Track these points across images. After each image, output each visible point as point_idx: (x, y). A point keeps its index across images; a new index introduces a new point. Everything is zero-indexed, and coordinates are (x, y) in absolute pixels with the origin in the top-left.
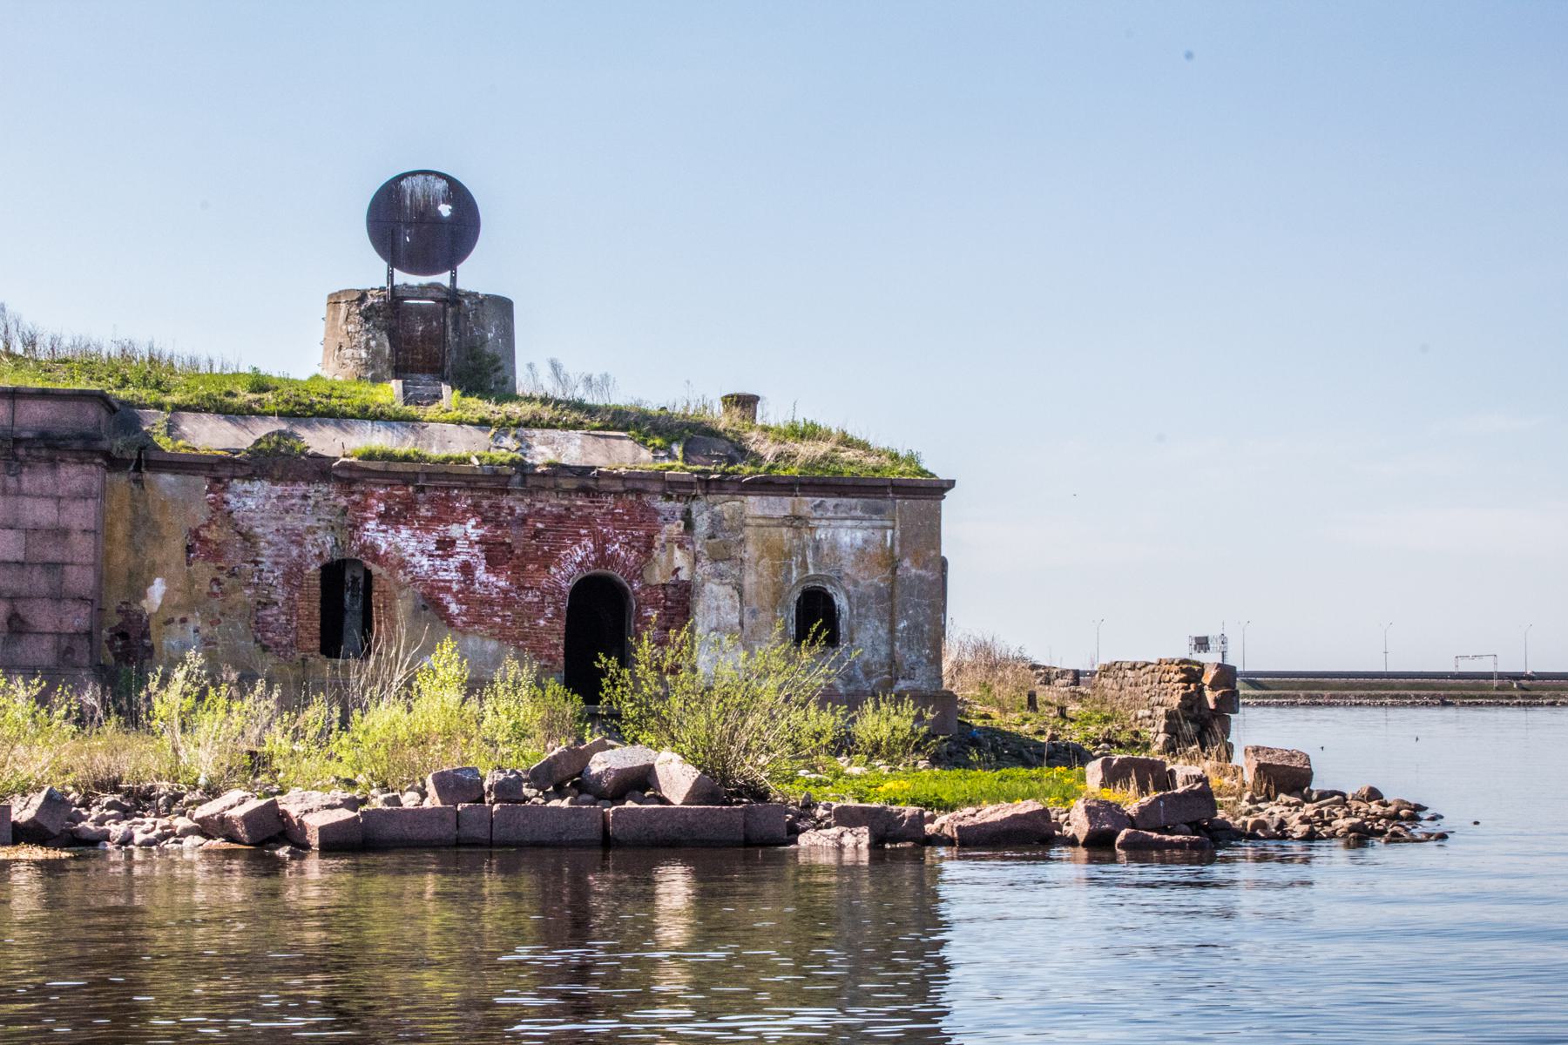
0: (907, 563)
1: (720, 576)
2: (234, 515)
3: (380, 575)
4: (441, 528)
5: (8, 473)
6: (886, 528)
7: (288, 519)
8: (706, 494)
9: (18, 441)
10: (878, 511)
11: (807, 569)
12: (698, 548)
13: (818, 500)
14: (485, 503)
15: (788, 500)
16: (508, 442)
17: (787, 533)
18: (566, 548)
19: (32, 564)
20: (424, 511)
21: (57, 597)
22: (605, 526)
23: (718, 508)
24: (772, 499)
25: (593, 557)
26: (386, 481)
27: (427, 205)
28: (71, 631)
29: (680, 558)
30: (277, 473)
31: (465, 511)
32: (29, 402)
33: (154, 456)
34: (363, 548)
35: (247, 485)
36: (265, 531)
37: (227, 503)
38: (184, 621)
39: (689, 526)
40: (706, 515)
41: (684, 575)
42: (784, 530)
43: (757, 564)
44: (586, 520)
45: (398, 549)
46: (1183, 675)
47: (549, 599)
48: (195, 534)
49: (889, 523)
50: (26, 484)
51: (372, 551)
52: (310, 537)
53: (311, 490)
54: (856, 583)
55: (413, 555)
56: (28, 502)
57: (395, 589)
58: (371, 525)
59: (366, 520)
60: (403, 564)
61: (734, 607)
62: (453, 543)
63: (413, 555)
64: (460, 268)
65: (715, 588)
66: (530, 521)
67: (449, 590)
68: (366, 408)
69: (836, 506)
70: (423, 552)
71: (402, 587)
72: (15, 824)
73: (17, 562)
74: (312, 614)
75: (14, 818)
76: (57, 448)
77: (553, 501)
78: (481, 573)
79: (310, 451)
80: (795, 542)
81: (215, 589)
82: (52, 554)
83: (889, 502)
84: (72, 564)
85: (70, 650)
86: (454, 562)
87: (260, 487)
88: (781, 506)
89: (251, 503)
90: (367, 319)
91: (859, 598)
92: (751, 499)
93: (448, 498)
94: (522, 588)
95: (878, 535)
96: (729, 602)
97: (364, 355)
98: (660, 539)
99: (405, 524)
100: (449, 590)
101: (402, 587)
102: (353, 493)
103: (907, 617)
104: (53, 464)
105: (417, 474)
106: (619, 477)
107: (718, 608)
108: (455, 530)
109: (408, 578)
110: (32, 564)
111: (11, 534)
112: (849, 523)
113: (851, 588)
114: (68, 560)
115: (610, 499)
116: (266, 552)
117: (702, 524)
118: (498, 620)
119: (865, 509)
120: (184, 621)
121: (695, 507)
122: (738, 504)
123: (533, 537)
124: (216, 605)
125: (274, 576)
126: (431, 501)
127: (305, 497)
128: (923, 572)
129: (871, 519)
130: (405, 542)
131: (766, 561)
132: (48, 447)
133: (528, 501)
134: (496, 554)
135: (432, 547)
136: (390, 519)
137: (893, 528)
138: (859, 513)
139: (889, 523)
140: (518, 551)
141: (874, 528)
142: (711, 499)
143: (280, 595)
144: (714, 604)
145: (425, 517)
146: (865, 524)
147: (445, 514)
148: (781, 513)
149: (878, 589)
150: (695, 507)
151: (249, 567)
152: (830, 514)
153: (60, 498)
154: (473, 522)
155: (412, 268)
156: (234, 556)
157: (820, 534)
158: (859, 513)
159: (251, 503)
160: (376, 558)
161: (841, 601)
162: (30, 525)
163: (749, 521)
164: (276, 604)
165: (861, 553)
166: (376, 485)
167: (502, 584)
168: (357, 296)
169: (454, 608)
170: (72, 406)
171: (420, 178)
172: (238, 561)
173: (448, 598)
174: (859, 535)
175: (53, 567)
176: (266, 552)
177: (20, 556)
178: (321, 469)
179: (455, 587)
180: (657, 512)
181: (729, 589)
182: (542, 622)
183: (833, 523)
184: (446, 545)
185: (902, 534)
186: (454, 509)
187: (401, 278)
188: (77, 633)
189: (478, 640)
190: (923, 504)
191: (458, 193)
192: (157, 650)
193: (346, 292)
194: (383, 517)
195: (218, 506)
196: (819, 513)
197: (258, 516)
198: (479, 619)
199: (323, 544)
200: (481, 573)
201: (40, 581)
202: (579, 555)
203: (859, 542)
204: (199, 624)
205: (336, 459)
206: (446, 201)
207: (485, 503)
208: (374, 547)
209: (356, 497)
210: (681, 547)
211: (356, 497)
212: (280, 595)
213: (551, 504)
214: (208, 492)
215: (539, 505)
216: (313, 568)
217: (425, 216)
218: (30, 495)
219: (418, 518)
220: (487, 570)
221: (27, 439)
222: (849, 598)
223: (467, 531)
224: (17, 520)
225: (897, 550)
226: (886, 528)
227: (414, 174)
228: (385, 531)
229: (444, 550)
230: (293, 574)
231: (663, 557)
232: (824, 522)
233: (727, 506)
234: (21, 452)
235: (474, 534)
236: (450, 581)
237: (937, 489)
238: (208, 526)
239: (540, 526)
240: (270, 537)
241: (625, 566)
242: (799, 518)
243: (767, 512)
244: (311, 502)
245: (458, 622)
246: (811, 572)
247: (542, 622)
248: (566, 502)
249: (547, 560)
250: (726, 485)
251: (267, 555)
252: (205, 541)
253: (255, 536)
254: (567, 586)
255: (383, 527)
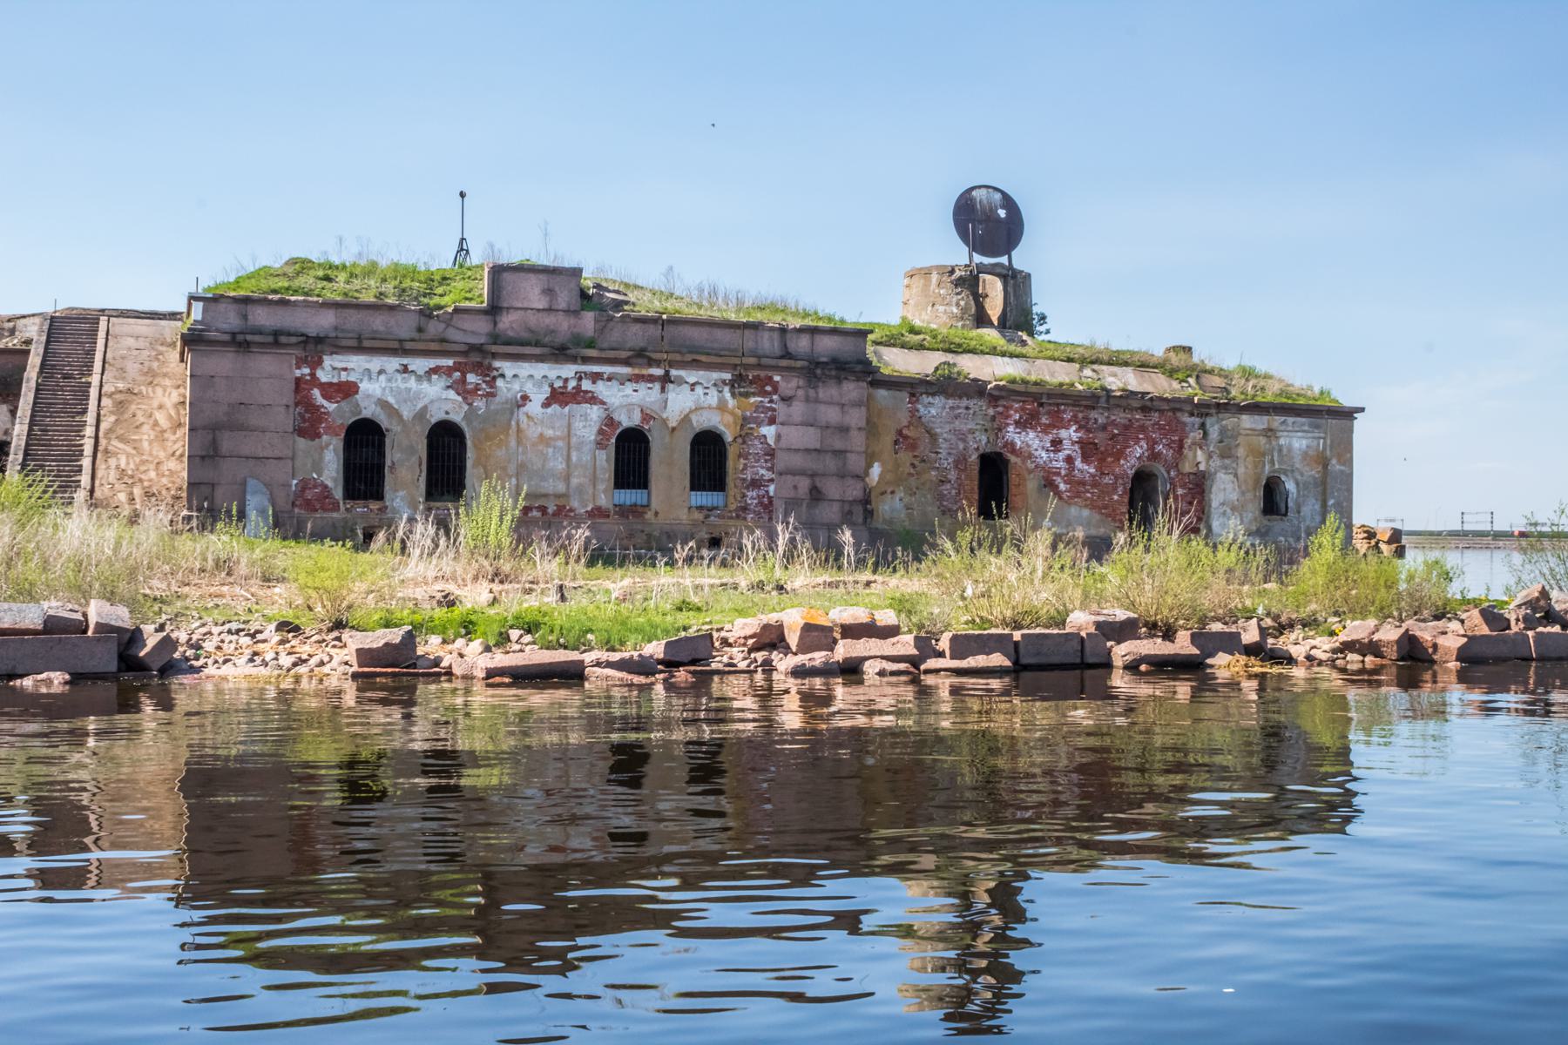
0: (1334, 461)
1: (1226, 468)
2: (923, 419)
3: (1016, 463)
4: (1055, 431)
5: (809, 386)
6: (1320, 438)
7: (957, 423)
8: (1217, 413)
9: (818, 364)
10: (1317, 427)
11: (1274, 464)
12: (1211, 449)
13: (1283, 418)
14: (1080, 415)
15: (1266, 418)
16: (1087, 372)
17: (1263, 440)
18: (1129, 447)
19: (826, 452)
20: (1044, 420)
21: (842, 475)
22: (1154, 432)
23: (1224, 422)
24: (1256, 417)
25: (1146, 454)
26: (1023, 399)
27: (991, 209)
28: (851, 499)
29: (1200, 456)
30: (950, 391)
31: (1070, 421)
32: (822, 337)
33: (878, 377)
34: (1006, 444)
35: (930, 399)
36: (942, 430)
37: (918, 411)
38: (893, 492)
39: (1205, 434)
40: (1216, 427)
41: (1202, 467)
42: (1261, 438)
43: (1245, 460)
44: (1143, 429)
45: (1028, 446)
46: (1366, 535)
47: (1120, 481)
48: (900, 433)
49: (1322, 435)
50: (821, 395)
51: (1010, 445)
52: (970, 436)
53: (971, 403)
54: (1302, 475)
55: (1036, 450)
56: (822, 408)
57: (1025, 473)
58: (1011, 429)
59: (1008, 425)
60: (1030, 456)
61: (1234, 489)
62: (1060, 442)
63: (1036, 450)
64: (1014, 253)
65: (1223, 476)
66: (1109, 428)
67: (1058, 474)
68: (995, 348)
69: (1294, 423)
70: (1043, 448)
71: (1030, 472)
72: (1245, 645)
73: (816, 450)
74: (973, 489)
75: (1244, 642)
76: (844, 369)
77: (1122, 415)
78: (1078, 463)
79: (971, 376)
80: (1267, 446)
81: (912, 471)
82: (838, 444)
83: (1324, 421)
84: (851, 452)
85: (850, 513)
86: (1061, 455)
87: (938, 401)
88: (1260, 422)
89: (933, 412)
90: (956, 286)
91: (1304, 485)
92: (1244, 417)
93: (1058, 411)
94: (1103, 474)
95: (1315, 442)
96: (1231, 485)
97: (955, 310)
98: (1188, 441)
99: (1031, 428)
100: (1058, 474)
101: (1030, 472)
102: (997, 406)
103: (1333, 498)
104: (839, 380)
105: (1042, 394)
106: (1166, 400)
107: (1225, 489)
108: (1063, 433)
109: (1033, 465)
110: (826, 452)
111: (811, 429)
112: (1299, 434)
113: (1299, 477)
114: (849, 448)
115: (1157, 415)
116: (944, 446)
117: (1214, 433)
118: (1089, 495)
119: (1310, 425)
120: (893, 492)
121: (1209, 421)
122: (1236, 420)
123: (1111, 439)
124: (913, 482)
125: (947, 462)
126: (1048, 413)
127: (967, 408)
128: (1342, 468)
129: (1313, 432)
130: (1031, 441)
131: (1250, 459)
132: (837, 369)
133: (1106, 414)
134: (1088, 449)
135: (1049, 445)
136: (1022, 425)
137: (1324, 438)
138: (1306, 428)
139: (1322, 435)
140: (1102, 449)
141: (1314, 438)
142: (1221, 416)
143: (952, 476)
144: (1222, 487)
145: (1045, 424)
146: (1310, 435)
147: (1058, 423)
148: (1262, 427)
149: (1315, 478)
150: (1209, 421)
151: (933, 455)
152: (1290, 428)
153: (843, 405)
154: (1074, 428)
155: (984, 253)
156: (924, 448)
157: (1282, 441)
158: (1306, 428)
159: (933, 412)
160: (1014, 451)
161: (1290, 486)
162: (824, 424)
163: (1242, 431)
164: (950, 482)
165: (1305, 455)
166: (1014, 401)
167: (1092, 470)
168: (950, 269)
169: (1062, 487)
170: (850, 339)
171: (983, 191)
172: (927, 452)
173: (1058, 480)
174: (1304, 442)
175: (840, 453)
176: (944, 446)
177: (818, 446)
178: (977, 389)
179: (1063, 472)
180: (1185, 424)
181: (1231, 477)
182: (1116, 497)
183: (1291, 434)
184: (1057, 444)
185: (1332, 442)
186: (1063, 419)
187: (978, 258)
188: (854, 501)
189: (1078, 508)
190: (1344, 422)
191: (1008, 202)
192: (875, 513)
193: (938, 267)
194: (1017, 423)
195: (914, 412)
196: (1282, 428)
197: (939, 420)
198: (1078, 495)
199: (981, 441)
200: (1078, 463)
201: (831, 464)
202: (1138, 451)
203: (1304, 446)
204: (902, 495)
205: (990, 382)
206: (1003, 207)
207: (1080, 415)
208: (1013, 444)
209: (1000, 409)
210: (1201, 448)
211: (1000, 409)
212: (952, 476)
213: (1120, 417)
214: (909, 403)
215: (1113, 418)
216: (974, 457)
217: (989, 217)
218: (825, 403)
219: (1040, 425)
220: (1082, 462)
221: (823, 363)
222: (1297, 484)
223: (1070, 434)
224: (815, 420)
225: (1328, 452)
226: (1320, 438)
227: (980, 187)
228: (1019, 433)
229: (1055, 446)
230: (960, 462)
231: (1190, 454)
232: (1286, 434)
233: (1230, 421)
234: (819, 371)
235: (1075, 436)
236: (1060, 468)
237: (1347, 415)
238: (908, 427)
239: (1116, 431)
240: (945, 435)
241: (1166, 461)
242: (1271, 430)
243: (1253, 426)
244: (971, 412)
245: (1064, 496)
246: (1277, 466)
247: (1116, 497)
248: (1129, 416)
249: (1119, 455)
250: (1229, 407)
251: (943, 447)
252: (906, 437)
253: (936, 434)
254: (1131, 472)
255: (1018, 430)
